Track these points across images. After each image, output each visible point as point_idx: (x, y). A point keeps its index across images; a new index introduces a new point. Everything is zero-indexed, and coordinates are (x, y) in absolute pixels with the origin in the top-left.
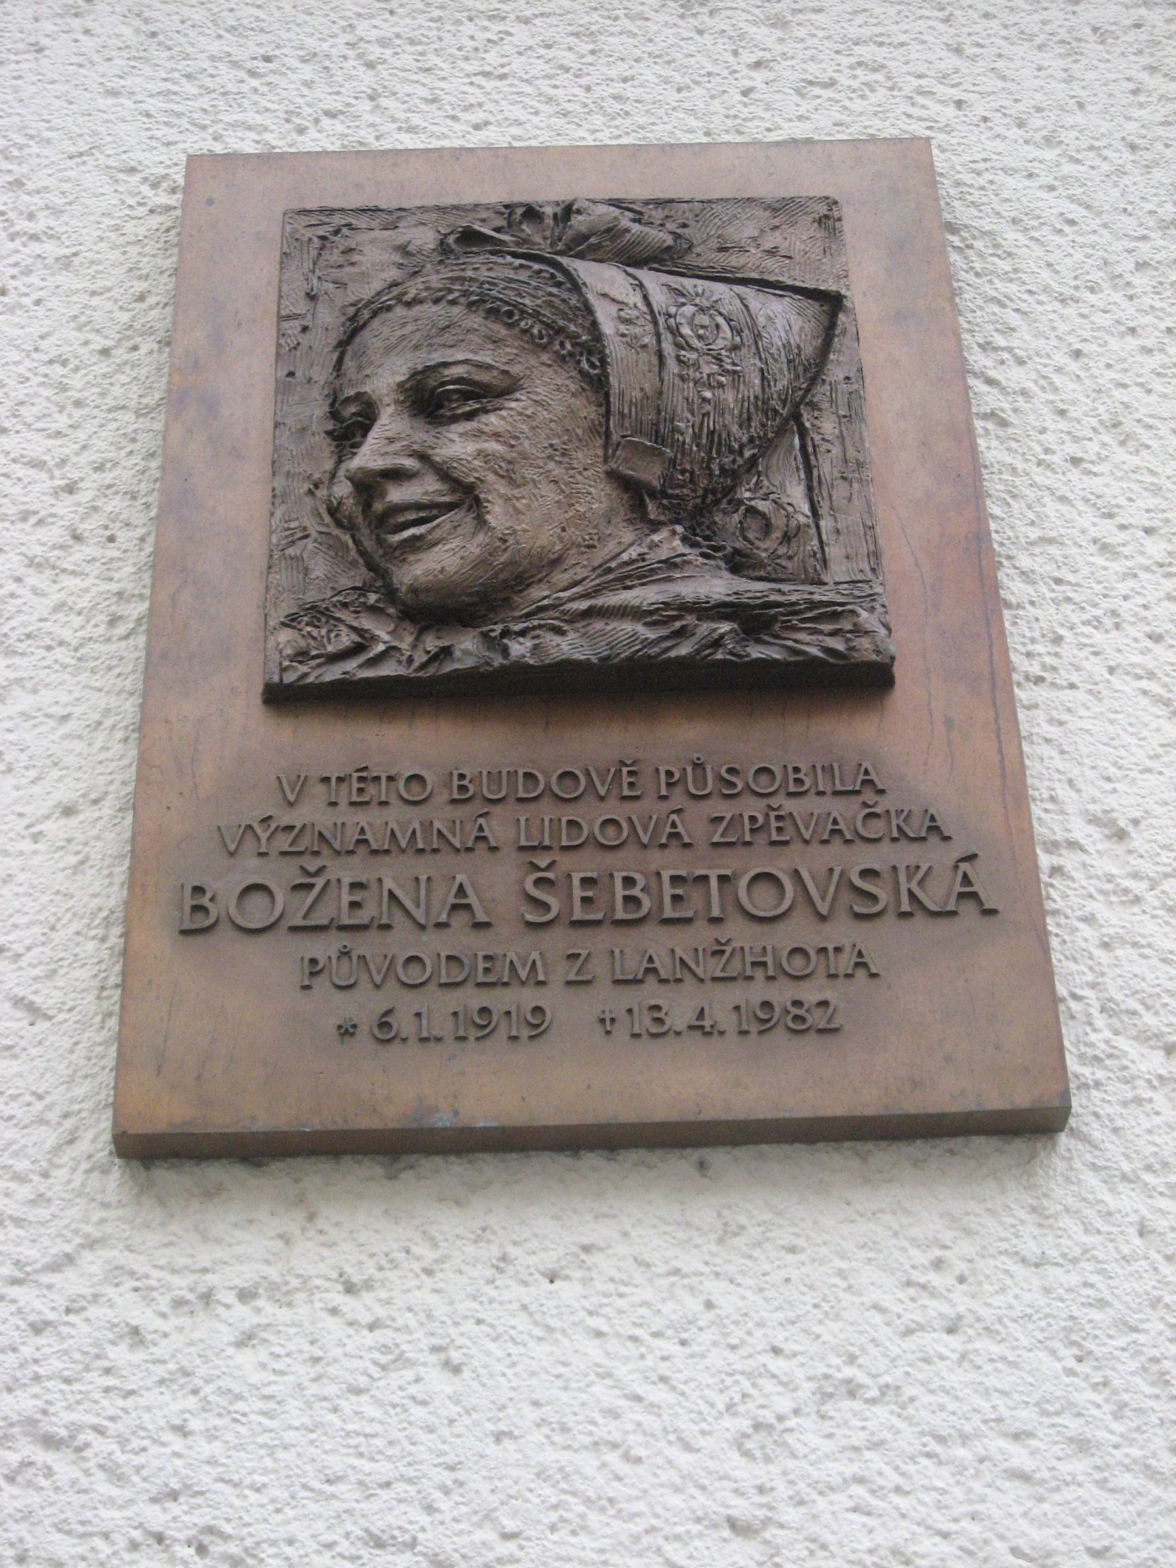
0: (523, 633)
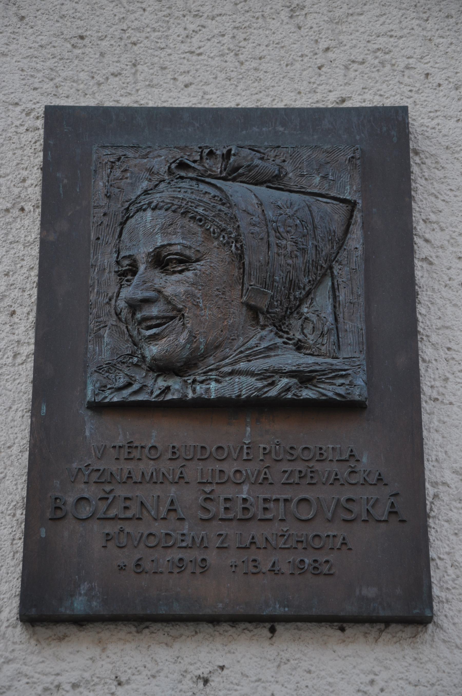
0: (202, 382)
